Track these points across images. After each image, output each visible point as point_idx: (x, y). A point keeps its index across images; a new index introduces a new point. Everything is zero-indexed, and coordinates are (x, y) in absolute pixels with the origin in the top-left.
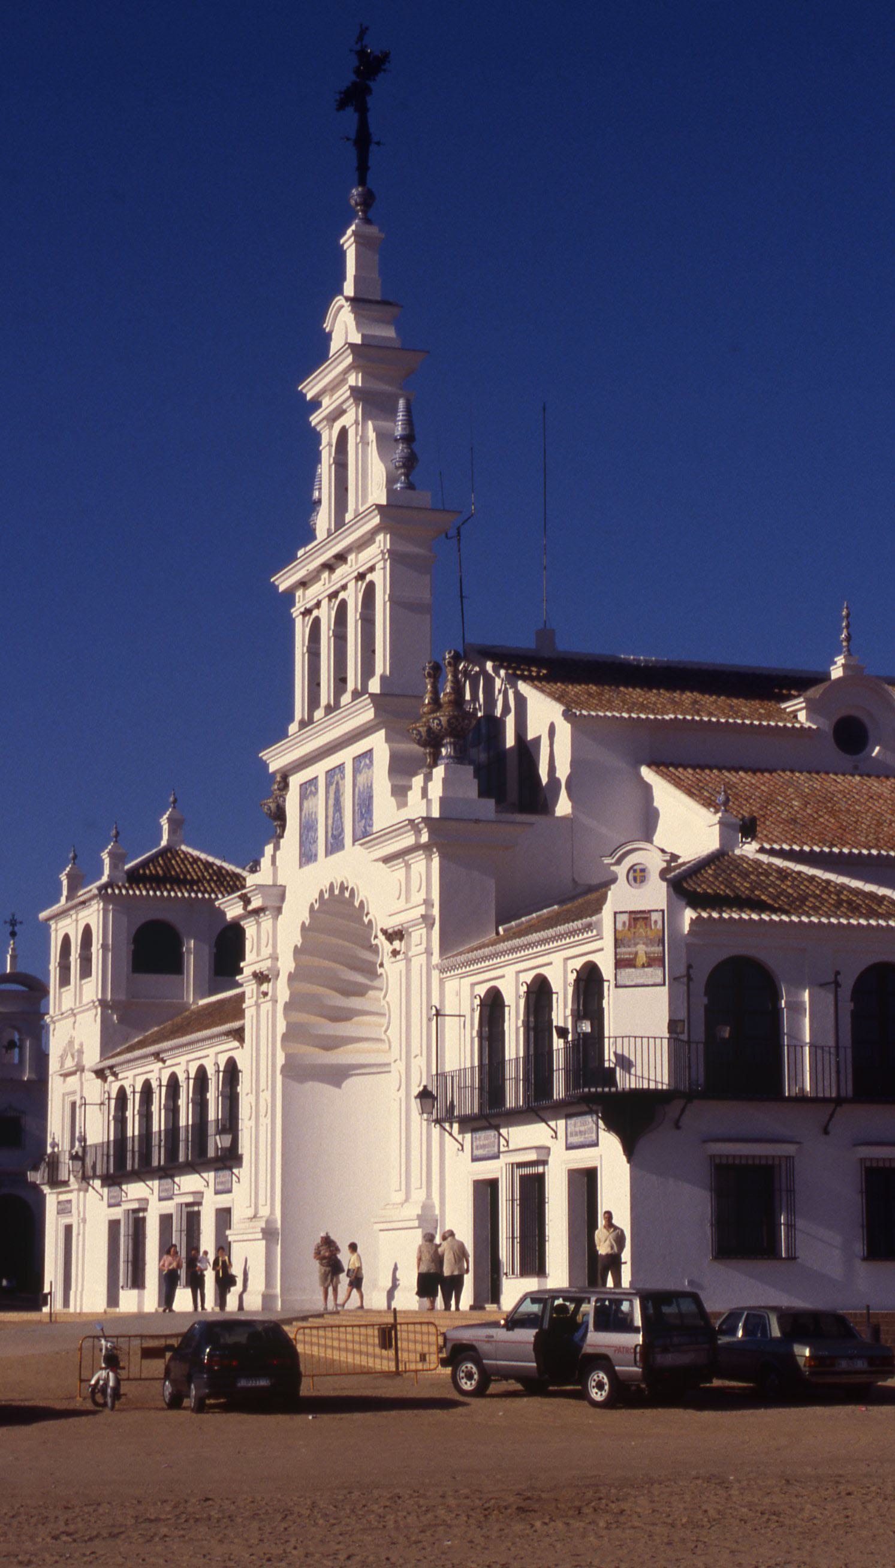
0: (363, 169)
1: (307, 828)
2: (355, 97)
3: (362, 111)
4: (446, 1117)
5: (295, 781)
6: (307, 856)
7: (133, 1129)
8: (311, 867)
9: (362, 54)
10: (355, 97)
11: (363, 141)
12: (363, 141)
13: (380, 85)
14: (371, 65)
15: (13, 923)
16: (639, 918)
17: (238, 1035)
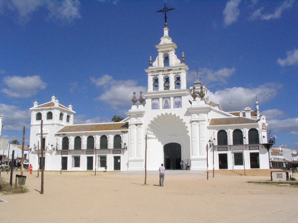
3: (165, 14)
9: (165, 7)
11: (166, 18)
12: (166, 18)
16: (264, 124)
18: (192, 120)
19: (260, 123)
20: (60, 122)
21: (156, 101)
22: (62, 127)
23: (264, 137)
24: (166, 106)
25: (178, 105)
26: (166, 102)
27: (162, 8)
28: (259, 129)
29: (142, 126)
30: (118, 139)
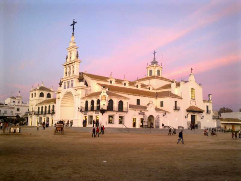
0: (73, 31)
1: (65, 86)
2: (73, 25)
3: (74, 26)
4: (81, 111)
5: (63, 82)
6: (65, 88)
7: (40, 110)
8: (65, 89)
9: (74, 22)
10: (73, 25)
11: (73, 29)
12: (73, 29)
13: (75, 24)
14: (74, 23)
15: (20, 91)
16: (104, 96)
17: (55, 103)
18: (76, 94)
19: (100, 96)
20: (41, 98)
21: (65, 84)
22: (42, 101)
23: (104, 105)
24: (68, 87)
25: (72, 85)
26: (69, 84)
27: (72, 23)
28: (100, 99)
29: (60, 99)
30: (53, 106)
